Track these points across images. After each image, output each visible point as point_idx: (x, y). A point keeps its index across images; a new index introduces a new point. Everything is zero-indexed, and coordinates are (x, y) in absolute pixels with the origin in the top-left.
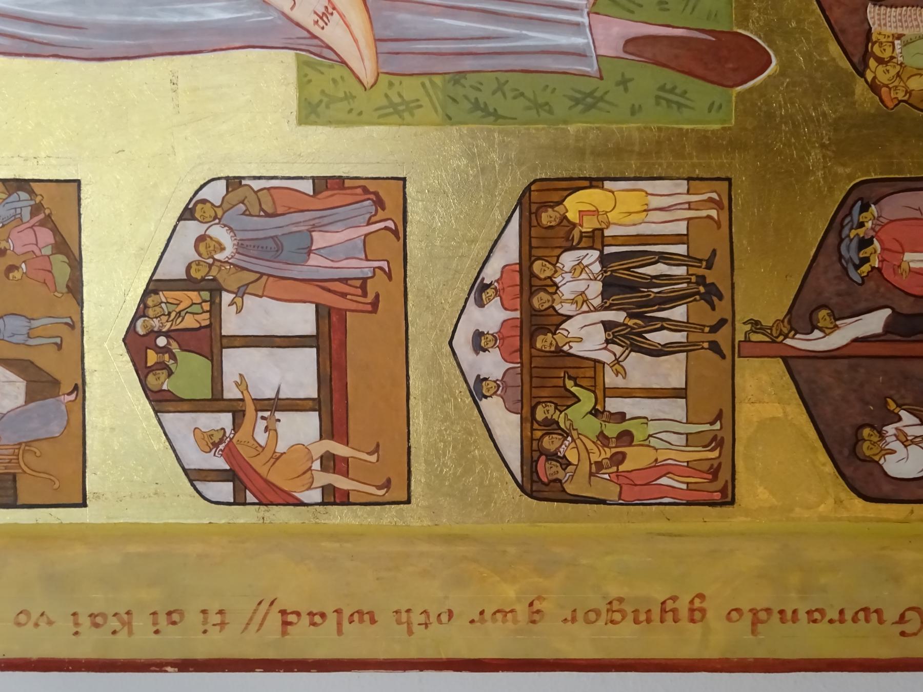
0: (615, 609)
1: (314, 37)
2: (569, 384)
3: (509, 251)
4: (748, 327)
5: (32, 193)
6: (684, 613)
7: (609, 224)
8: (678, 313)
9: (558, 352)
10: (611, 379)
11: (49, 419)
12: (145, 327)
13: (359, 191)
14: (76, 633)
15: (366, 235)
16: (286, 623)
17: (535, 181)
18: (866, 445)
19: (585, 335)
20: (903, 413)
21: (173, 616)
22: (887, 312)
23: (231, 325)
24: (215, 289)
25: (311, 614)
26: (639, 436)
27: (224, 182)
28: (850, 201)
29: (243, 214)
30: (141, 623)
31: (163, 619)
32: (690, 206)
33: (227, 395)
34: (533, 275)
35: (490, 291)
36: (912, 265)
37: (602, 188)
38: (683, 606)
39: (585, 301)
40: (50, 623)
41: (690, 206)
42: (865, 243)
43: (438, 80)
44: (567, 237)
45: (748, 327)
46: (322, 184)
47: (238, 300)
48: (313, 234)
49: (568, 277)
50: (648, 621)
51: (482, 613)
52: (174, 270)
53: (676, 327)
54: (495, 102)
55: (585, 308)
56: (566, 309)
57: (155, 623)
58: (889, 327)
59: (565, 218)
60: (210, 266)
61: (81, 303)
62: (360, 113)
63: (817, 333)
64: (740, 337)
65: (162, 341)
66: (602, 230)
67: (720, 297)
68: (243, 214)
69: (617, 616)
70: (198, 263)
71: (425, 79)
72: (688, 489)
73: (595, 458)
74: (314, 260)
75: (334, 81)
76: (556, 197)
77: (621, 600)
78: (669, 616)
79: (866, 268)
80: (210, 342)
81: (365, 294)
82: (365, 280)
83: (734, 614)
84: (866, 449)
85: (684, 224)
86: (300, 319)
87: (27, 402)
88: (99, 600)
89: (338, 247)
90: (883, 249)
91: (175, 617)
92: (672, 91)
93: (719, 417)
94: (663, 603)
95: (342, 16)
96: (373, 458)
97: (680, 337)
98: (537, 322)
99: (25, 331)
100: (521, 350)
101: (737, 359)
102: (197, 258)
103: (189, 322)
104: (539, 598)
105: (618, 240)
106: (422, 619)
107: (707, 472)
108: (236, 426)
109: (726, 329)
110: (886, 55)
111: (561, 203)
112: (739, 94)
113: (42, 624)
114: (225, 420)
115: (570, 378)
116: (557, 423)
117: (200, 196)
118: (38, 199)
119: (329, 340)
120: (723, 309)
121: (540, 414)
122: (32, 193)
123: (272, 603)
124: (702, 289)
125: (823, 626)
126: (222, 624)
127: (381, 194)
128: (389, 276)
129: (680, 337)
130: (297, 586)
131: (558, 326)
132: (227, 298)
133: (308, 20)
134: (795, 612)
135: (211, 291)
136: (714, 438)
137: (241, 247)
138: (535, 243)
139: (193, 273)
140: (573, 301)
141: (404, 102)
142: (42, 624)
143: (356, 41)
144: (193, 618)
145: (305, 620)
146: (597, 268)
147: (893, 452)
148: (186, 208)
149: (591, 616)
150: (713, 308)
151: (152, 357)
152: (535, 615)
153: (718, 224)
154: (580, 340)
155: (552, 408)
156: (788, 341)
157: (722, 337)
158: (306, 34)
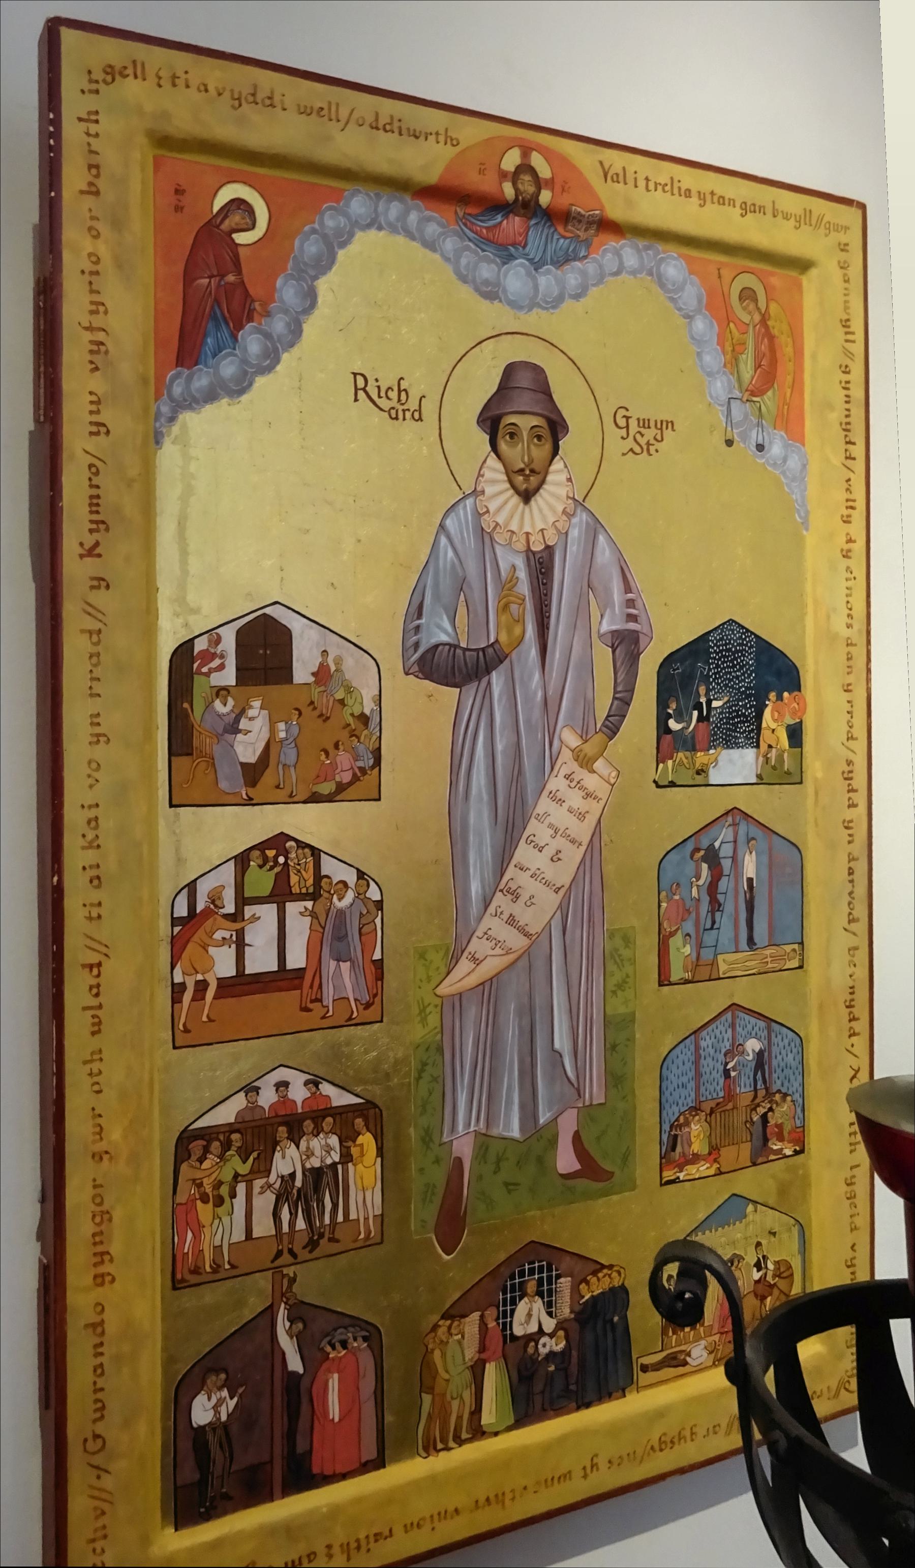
0: (103, 1216)
1: (463, 952)
2: (255, 1154)
3: (340, 1098)
4: (292, 1275)
5: (373, 768)
6: (101, 1269)
7: (355, 1165)
8: (301, 1224)
9: (276, 1143)
10: (258, 1183)
11: (230, 781)
12: (291, 847)
13: (375, 991)
14: (83, 806)
15: (348, 999)
16: (91, 967)
17: (381, 1111)
18: (214, 1378)
19: (287, 1161)
20: (236, 1399)
21: (96, 881)
22: (301, 1371)
23: (293, 908)
24: (314, 896)
25: (98, 986)
26: (219, 1210)
27: (379, 898)
28: (370, 1328)
29: (361, 913)
30: (91, 856)
31: (94, 872)
32: (366, 1219)
33: (246, 908)
34: (324, 1118)
35: (314, 1089)
36: (331, 1381)
37: (377, 1157)
38: (106, 1268)
39: (308, 1157)
40: (91, 786)
41: (366, 1219)
42: (344, 1344)
43: (439, 1037)
44: (348, 1137)
45: (292, 1275)
46: (379, 965)
47: (308, 913)
48: (348, 963)
49: (323, 1142)
50: (95, 1244)
51: (100, 1116)
52: (328, 866)
53: (292, 1224)
54: (426, 1076)
55: (304, 1157)
56: (303, 1144)
57: (91, 867)
58: (294, 1374)
59: (359, 1134)
60: (329, 892)
61: (305, 802)
62: (420, 988)
63: (288, 1324)
64: (285, 1271)
65: (281, 860)
66: (352, 1161)
67: (311, 1252)
68: (361, 913)
69: (98, 1219)
70: (331, 884)
71: (439, 1029)
72: (184, 1254)
73: (206, 1181)
74: (333, 964)
75: (438, 968)
76: (371, 1126)
77: (110, 1220)
78: (98, 1259)
79: (328, 1349)
80: (281, 895)
81: (312, 1001)
82: (320, 1000)
83: (100, 1308)
84: (212, 1379)
85: (356, 1217)
86: (296, 959)
87: (242, 764)
88: (107, 824)
89: (342, 981)
90: (340, 1358)
91: (96, 882)
92: (433, 1194)
93: (233, 1267)
94: (108, 1253)
95: (473, 970)
96: (205, 1019)
97: (285, 1228)
98: (294, 1123)
99: (288, 763)
100: (277, 1116)
101: (271, 1271)
102: (334, 882)
103: (294, 879)
104: (111, 1158)
105: (346, 1172)
106: (95, 1071)
107: (196, 1266)
108: (226, 916)
109: (290, 1260)
110: (453, 1331)
111: (368, 1130)
112: (431, 1238)
113: (91, 781)
114: (230, 908)
115: (259, 1155)
116: (229, 1150)
117: (372, 883)
118: (369, 772)
119: (284, 978)
120: (303, 1255)
121: (235, 1137)
122: (373, 768)
123: (106, 955)
124: (315, 1238)
125: (91, 1377)
126: (90, 918)
127: (372, 1008)
128: (324, 1017)
129: (285, 1228)
130: (119, 973)
131: (292, 1140)
132: (309, 904)
133: (471, 948)
134: (102, 1354)
135: (313, 893)
136: (219, 1266)
137: (341, 913)
138: (344, 1116)
139: (325, 880)
140: (308, 1148)
141: (426, 1016)
142: (91, 781)
143: (459, 981)
144: (95, 896)
145: (94, 982)
146: (329, 1161)
147: (209, 1399)
148: (364, 874)
149: (98, 1200)
150: (304, 1248)
151: (271, 853)
152: (98, 1157)
153: (356, 1240)
154: (284, 1157)
155: (239, 1144)
156: (283, 1305)
157: (286, 1258)
158: (464, 947)
